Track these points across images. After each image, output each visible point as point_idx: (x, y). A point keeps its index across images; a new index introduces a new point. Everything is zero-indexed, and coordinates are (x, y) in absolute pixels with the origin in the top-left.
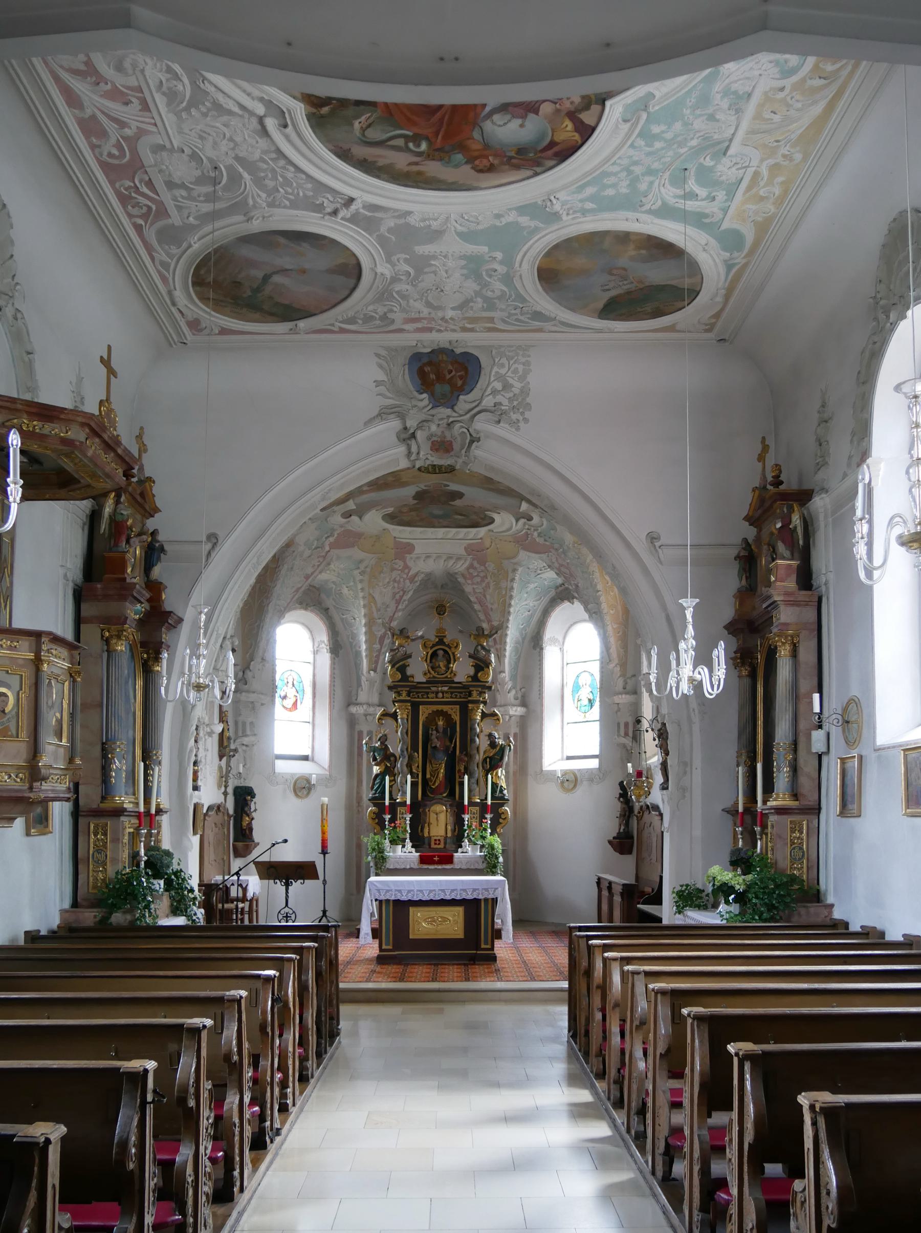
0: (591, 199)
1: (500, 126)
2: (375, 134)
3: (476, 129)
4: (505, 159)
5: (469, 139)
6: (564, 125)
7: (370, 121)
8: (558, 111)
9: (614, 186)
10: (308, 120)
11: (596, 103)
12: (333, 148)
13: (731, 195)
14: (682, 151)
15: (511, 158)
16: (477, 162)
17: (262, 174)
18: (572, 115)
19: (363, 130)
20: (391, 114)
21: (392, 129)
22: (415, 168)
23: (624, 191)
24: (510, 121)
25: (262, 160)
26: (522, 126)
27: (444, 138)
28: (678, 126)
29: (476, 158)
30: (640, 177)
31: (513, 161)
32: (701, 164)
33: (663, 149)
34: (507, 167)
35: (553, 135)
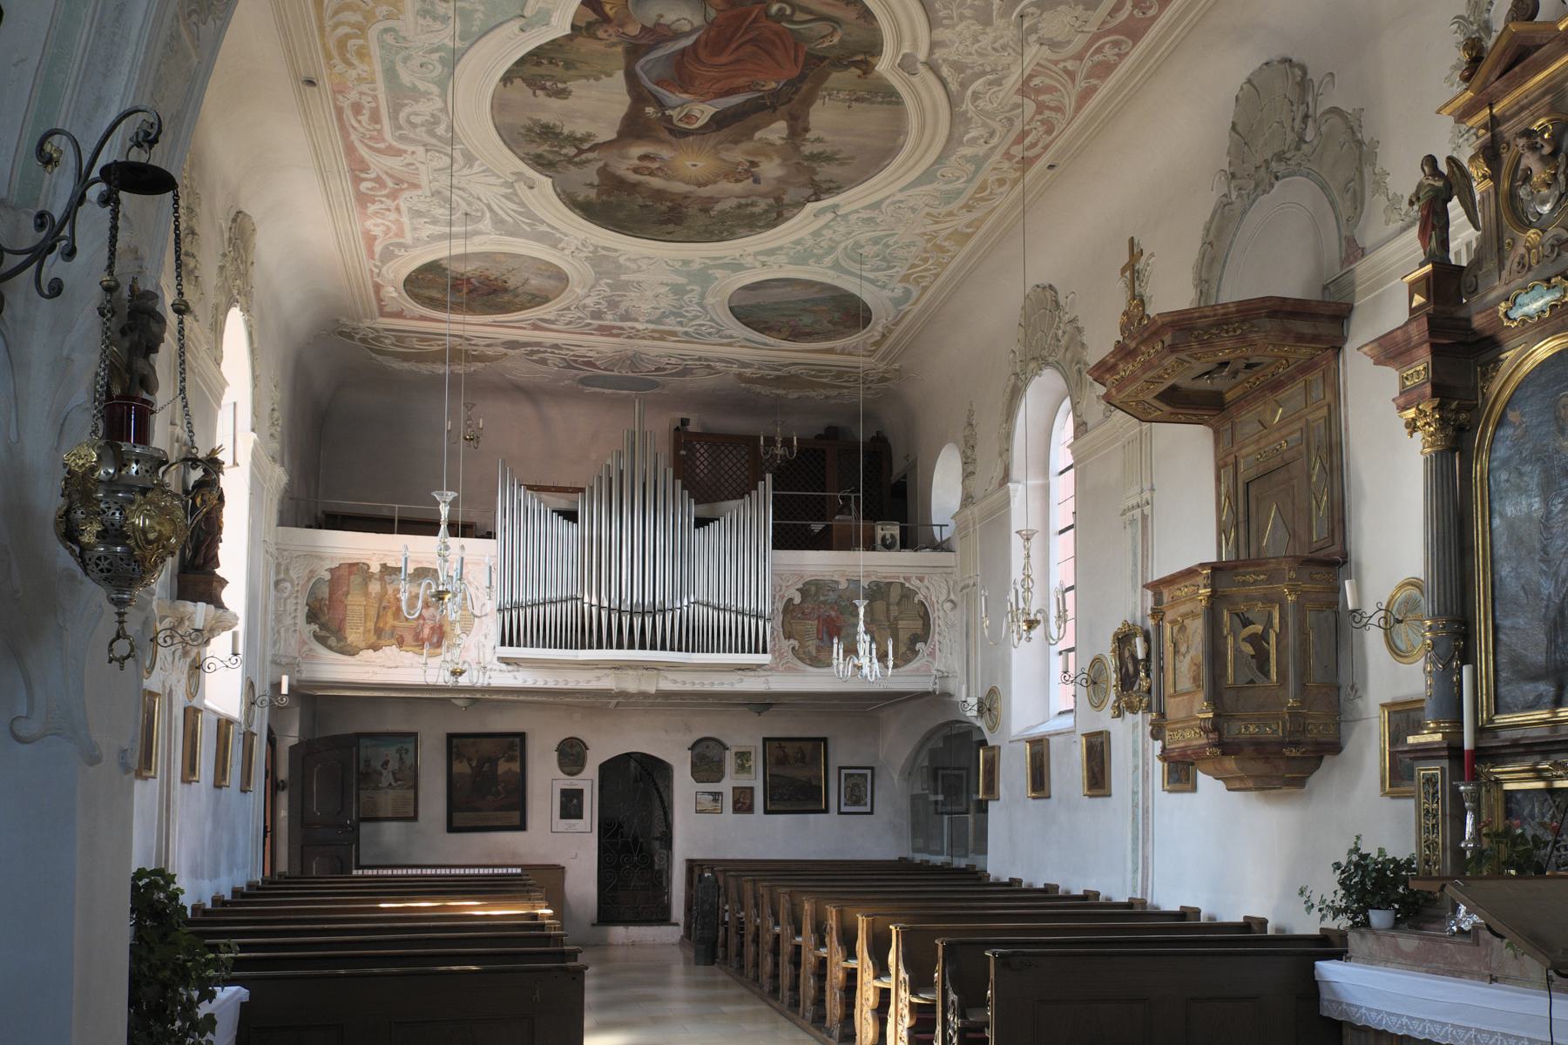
1: (685, 19)
2: (821, 28)
5: (722, 11)
6: (613, 11)
8: (621, 26)
10: (882, 51)
18: (606, 20)
19: (832, 35)
20: (796, 44)
21: (802, 31)
25: (962, 17)
26: (661, 16)
27: (750, 14)
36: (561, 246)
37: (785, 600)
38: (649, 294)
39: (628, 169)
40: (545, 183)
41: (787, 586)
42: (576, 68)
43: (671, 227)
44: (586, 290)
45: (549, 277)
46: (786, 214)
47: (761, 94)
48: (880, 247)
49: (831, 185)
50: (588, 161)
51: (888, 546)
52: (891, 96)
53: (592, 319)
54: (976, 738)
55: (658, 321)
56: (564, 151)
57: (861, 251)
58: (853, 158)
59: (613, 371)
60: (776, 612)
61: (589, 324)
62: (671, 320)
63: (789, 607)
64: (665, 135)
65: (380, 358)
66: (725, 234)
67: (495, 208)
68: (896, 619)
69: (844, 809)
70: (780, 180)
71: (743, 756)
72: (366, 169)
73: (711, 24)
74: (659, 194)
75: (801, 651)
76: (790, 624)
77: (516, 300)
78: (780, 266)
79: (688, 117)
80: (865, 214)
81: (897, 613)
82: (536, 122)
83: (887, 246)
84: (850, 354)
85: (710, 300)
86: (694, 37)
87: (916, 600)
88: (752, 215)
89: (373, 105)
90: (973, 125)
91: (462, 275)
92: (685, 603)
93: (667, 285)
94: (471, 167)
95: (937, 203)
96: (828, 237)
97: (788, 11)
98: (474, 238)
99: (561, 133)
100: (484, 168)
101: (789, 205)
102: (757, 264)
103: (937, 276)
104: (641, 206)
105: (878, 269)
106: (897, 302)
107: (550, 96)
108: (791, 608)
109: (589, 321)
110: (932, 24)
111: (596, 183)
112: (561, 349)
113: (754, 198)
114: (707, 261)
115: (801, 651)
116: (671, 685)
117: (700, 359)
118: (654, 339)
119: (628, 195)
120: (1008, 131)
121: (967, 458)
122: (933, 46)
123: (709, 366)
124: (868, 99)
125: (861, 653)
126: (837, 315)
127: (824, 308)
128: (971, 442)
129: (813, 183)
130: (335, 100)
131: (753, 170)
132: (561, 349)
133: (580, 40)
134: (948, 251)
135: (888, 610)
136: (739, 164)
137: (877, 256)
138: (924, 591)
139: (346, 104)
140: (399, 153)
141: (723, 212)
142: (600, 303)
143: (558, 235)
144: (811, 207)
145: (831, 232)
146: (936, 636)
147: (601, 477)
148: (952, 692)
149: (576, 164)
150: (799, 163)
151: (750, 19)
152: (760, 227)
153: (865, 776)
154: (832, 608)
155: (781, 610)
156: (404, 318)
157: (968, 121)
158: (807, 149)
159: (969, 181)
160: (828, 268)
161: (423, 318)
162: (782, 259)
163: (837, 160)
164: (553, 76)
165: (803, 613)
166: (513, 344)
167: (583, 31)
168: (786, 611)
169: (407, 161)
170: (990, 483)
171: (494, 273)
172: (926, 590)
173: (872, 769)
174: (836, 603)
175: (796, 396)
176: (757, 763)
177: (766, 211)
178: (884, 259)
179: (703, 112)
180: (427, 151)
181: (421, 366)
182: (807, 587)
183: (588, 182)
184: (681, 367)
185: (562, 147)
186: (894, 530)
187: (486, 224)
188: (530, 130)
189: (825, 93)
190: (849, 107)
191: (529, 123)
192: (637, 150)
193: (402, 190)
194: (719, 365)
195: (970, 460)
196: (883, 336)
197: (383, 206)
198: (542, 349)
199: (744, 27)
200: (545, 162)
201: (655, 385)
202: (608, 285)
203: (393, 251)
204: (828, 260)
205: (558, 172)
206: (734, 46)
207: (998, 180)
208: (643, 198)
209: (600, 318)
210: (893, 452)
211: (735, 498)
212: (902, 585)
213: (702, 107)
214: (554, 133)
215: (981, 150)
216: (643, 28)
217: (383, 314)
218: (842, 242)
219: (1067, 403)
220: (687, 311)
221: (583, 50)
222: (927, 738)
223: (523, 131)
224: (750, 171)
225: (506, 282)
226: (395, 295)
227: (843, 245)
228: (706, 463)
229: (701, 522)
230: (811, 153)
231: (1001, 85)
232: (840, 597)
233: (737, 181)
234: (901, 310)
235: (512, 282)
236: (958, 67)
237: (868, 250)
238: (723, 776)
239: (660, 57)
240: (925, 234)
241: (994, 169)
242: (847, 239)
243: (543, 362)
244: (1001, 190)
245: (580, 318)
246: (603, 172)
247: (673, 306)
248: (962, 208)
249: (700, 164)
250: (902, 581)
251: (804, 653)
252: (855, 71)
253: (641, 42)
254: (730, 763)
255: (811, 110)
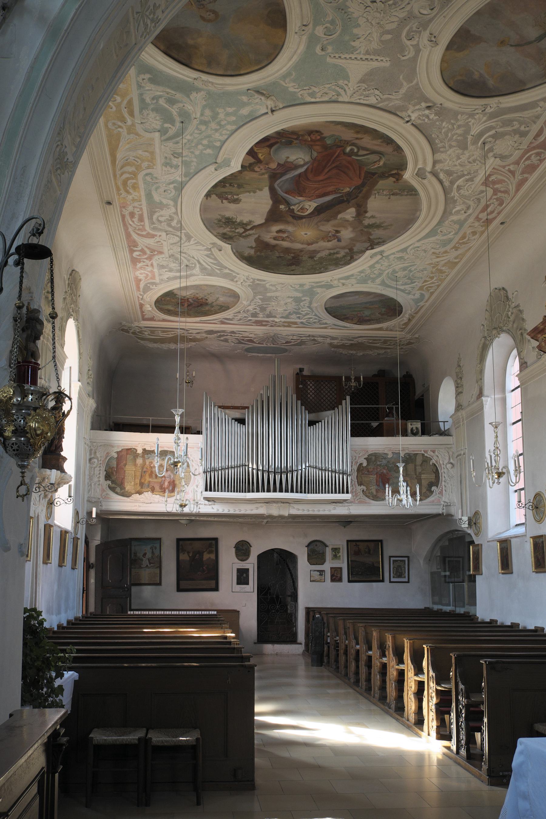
0: (244, 105)
1: (301, 158)
2: (373, 157)
3: (314, 157)
4: (300, 138)
5: (320, 152)
7: (374, 164)
8: (267, 164)
9: (228, 114)
10: (407, 168)
11: (246, 166)
12: (403, 153)
13: (142, 100)
14: (188, 137)
15: (296, 139)
16: (319, 137)
17: (458, 138)
18: (259, 161)
19: (379, 161)
20: (360, 167)
22: (359, 136)
23: (220, 110)
24: (294, 161)
25: (451, 147)
26: (288, 158)
27: (335, 153)
28: (197, 153)
29: (318, 140)
30: (211, 120)
31: (295, 137)
32: (173, 125)
33: (202, 139)
34: (300, 133)
35: (270, 151)
36: (235, 280)
37: (358, 464)
38: (282, 303)
39: (271, 238)
40: (227, 247)
41: (359, 457)
42: (244, 187)
43: (293, 267)
44: (249, 302)
45: (230, 296)
46: (355, 257)
47: (341, 194)
48: (407, 272)
49: (380, 240)
50: (250, 235)
51: (414, 434)
52: (412, 191)
53: (252, 317)
54: (468, 539)
55: (287, 317)
56: (237, 231)
57: (396, 275)
58: (391, 225)
59: (263, 344)
60: (353, 471)
61: (250, 320)
62: (294, 316)
63: (360, 469)
64: (290, 219)
65: (142, 342)
66: (323, 269)
67: (202, 262)
68: (420, 474)
69: (392, 580)
70: (352, 239)
71: (336, 550)
72: (136, 245)
73: (314, 160)
74: (287, 250)
75: (367, 492)
76: (361, 477)
77: (212, 309)
78: (353, 285)
79: (302, 209)
80: (398, 255)
81: (420, 471)
82: (223, 216)
83: (411, 271)
84: (391, 330)
85: (314, 305)
86: (305, 167)
87: (431, 463)
88: (337, 259)
89: (140, 213)
90: (458, 204)
91: (184, 297)
92: (304, 467)
93: (291, 297)
94: (189, 241)
95: (438, 246)
96: (378, 268)
97: (356, 150)
98: (191, 278)
99: (236, 222)
100: (196, 241)
101: (357, 252)
102: (340, 284)
103: (438, 286)
104: (278, 257)
105: (406, 284)
106: (417, 301)
107: (230, 203)
108: (362, 468)
109: (250, 318)
110: (434, 151)
111: (254, 246)
112: (236, 333)
113: (338, 250)
114: (313, 284)
115: (367, 492)
116: (297, 511)
117: (309, 336)
118: (285, 326)
119: (271, 251)
120: (478, 206)
121: (458, 384)
122: (435, 163)
123: (314, 340)
124: (400, 193)
125: (402, 492)
126: (384, 310)
127: (376, 306)
128: (460, 376)
129: (370, 240)
130: (121, 211)
131: (337, 235)
132: (236, 333)
133: (246, 172)
134: (445, 272)
135: (415, 469)
136: (330, 232)
137: (405, 277)
138: (435, 458)
139: (126, 213)
140: (153, 236)
141: (321, 258)
142: (256, 309)
143: (234, 274)
144: (369, 253)
145: (380, 265)
146: (443, 483)
147: (258, 400)
148: (453, 514)
149: (244, 237)
150: (362, 230)
151: (335, 156)
152: (342, 265)
153: (404, 561)
154: (384, 468)
155: (356, 470)
156: (155, 321)
157: (455, 201)
158: (366, 222)
159: (456, 234)
160: (379, 285)
161: (164, 320)
162: (353, 281)
163: (382, 227)
164: (232, 192)
165: (368, 471)
166: (211, 332)
167: (247, 168)
168: (358, 470)
169: (157, 240)
170: (472, 397)
171: (200, 296)
172: (437, 458)
173: (408, 557)
174: (386, 465)
175: (361, 354)
176: (344, 554)
177: (344, 256)
178: (409, 278)
179: (310, 206)
180: (167, 234)
181: (163, 345)
182: (370, 457)
183: (250, 246)
184: (299, 341)
185: (236, 229)
186: (417, 425)
187: (197, 270)
188: (220, 221)
189: (376, 192)
190: (389, 198)
191: (219, 217)
192: (275, 228)
193: (154, 255)
194: (319, 339)
195: (459, 386)
196: (409, 320)
197: (145, 264)
198: (225, 334)
199: (332, 160)
200: (227, 237)
201: (285, 351)
202: (260, 299)
203: (149, 286)
204: (378, 281)
205: (234, 242)
206: (326, 170)
207: (472, 232)
208: (279, 253)
209: (256, 317)
210: (416, 381)
211: (329, 410)
212: (423, 455)
213: (309, 203)
214: (232, 222)
215: (462, 217)
216: (279, 164)
217: (144, 319)
218: (385, 270)
219: (515, 352)
220: (302, 311)
221: (247, 178)
222: (439, 540)
223: (216, 221)
224: (336, 236)
225: (207, 300)
226: (150, 309)
227: (386, 272)
228: (313, 392)
229: (312, 423)
230: (369, 224)
231: (473, 181)
232: (388, 462)
233: (329, 241)
234: (419, 305)
235: (210, 300)
236: (449, 173)
237: (400, 274)
238: (325, 561)
239: (288, 179)
240: (432, 264)
241: (470, 226)
242: (389, 268)
243: (226, 341)
244: (474, 237)
245: (245, 317)
246: (258, 240)
247: (295, 309)
248: (452, 249)
249: (309, 233)
250: (423, 453)
251: (369, 493)
252: (392, 179)
253: (278, 172)
254: (329, 553)
255: (368, 201)
